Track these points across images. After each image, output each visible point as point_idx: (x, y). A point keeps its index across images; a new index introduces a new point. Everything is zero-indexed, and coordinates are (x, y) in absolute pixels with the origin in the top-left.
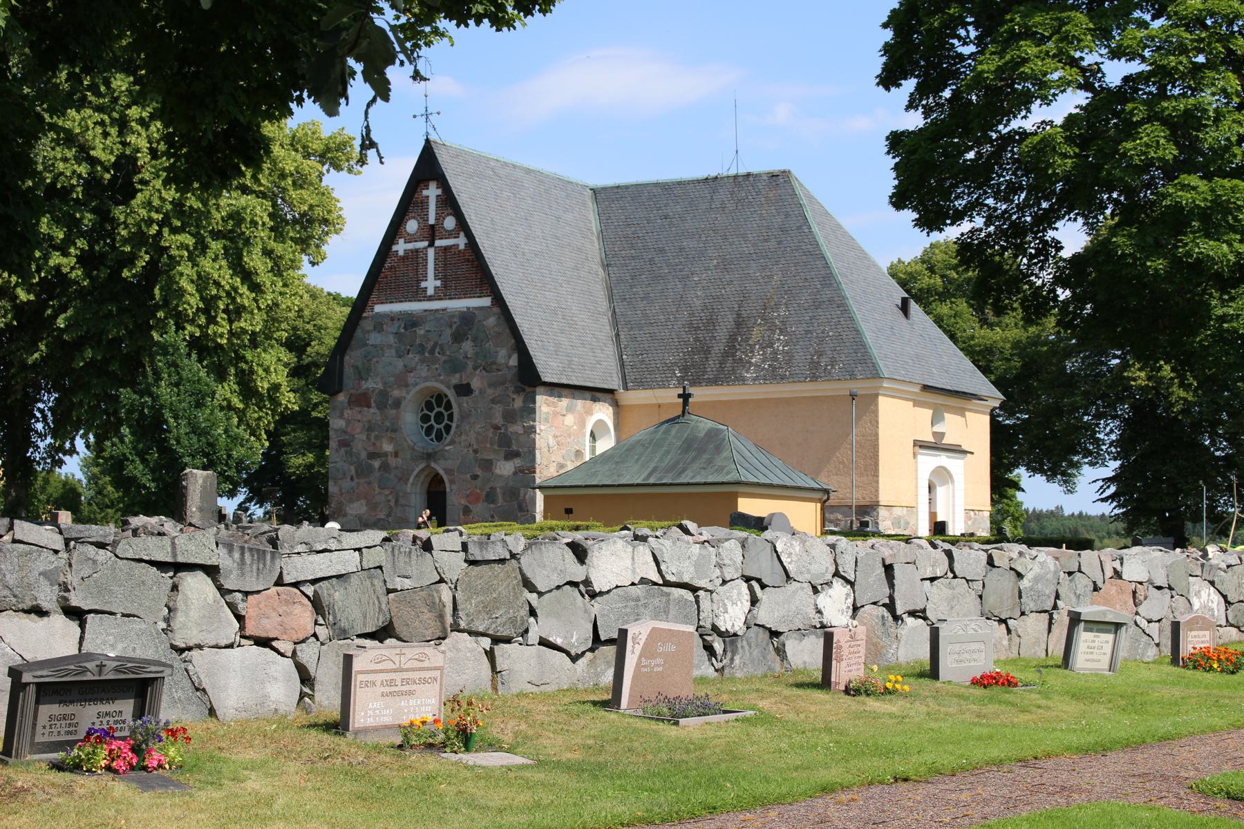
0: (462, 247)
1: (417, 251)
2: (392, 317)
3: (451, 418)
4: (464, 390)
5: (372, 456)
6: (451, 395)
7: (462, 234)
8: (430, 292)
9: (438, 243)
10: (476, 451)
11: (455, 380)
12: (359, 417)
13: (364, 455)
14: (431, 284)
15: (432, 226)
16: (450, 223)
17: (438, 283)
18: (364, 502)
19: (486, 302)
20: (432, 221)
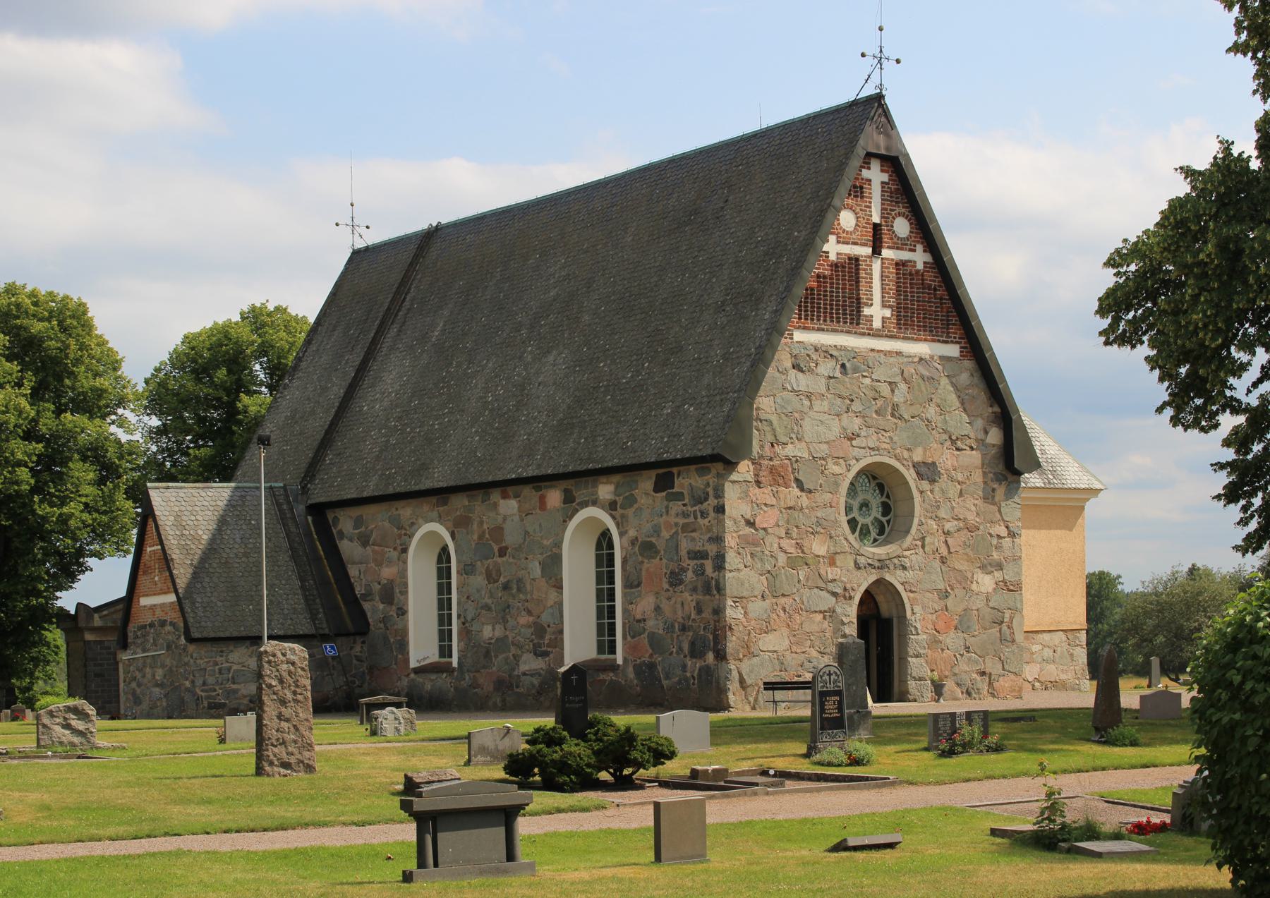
0: (920, 266)
1: (857, 260)
2: (827, 353)
3: (849, 509)
4: (928, 471)
5: (792, 563)
6: (910, 475)
7: (919, 248)
8: (877, 324)
9: (886, 253)
10: (943, 560)
11: (918, 456)
12: (773, 501)
13: (782, 558)
14: (877, 312)
15: (876, 228)
16: (902, 227)
17: (888, 313)
18: (785, 631)
19: (953, 350)
20: (876, 219)
